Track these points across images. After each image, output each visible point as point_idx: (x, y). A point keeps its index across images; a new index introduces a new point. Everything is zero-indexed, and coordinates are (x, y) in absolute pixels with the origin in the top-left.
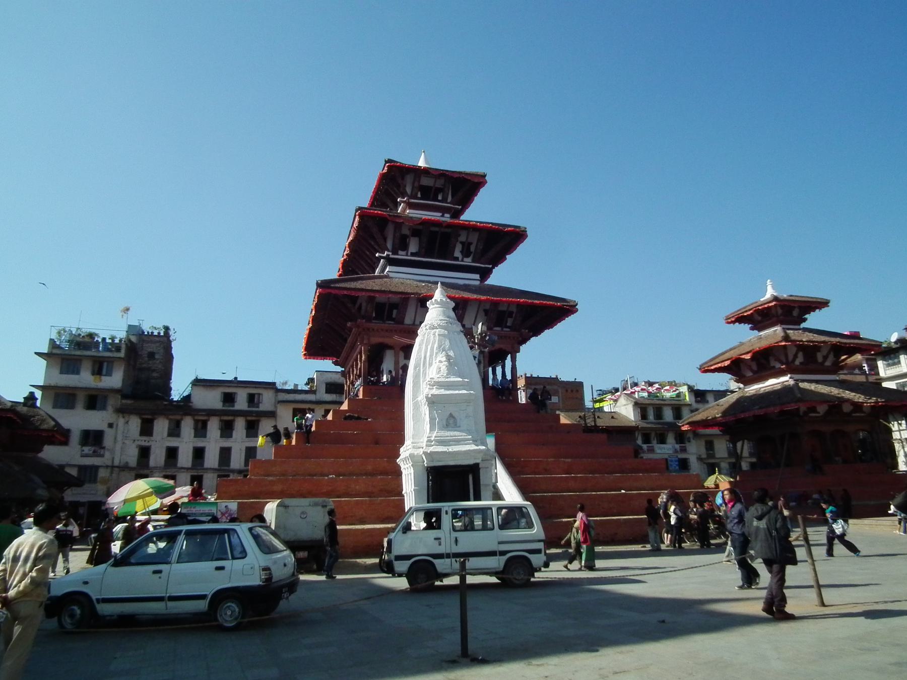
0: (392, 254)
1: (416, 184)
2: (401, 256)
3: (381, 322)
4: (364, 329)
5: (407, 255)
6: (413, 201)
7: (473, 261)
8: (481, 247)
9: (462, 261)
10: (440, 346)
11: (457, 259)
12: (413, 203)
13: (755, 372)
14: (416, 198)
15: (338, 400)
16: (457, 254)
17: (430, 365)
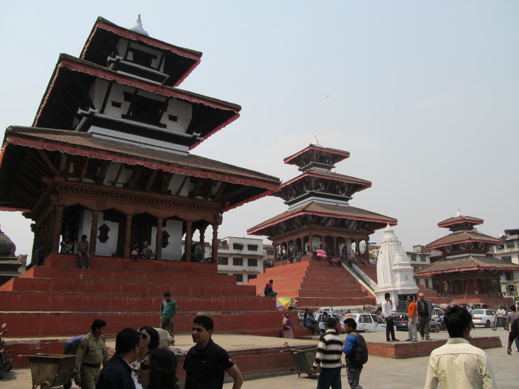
0: (314, 192)
1: (319, 156)
2: (318, 192)
3: (317, 225)
4: (311, 228)
5: (320, 192)
6: (317, 163)
7: (346, 195)
8: (351, 189)
9: (342, 195)
10: (396, 249)
11: (339, 194)
12: (317, 164)
13: (451, 251)
14: (318, 162)
15: (239, 253)
16: (340, 192)
17: (394, 256)
